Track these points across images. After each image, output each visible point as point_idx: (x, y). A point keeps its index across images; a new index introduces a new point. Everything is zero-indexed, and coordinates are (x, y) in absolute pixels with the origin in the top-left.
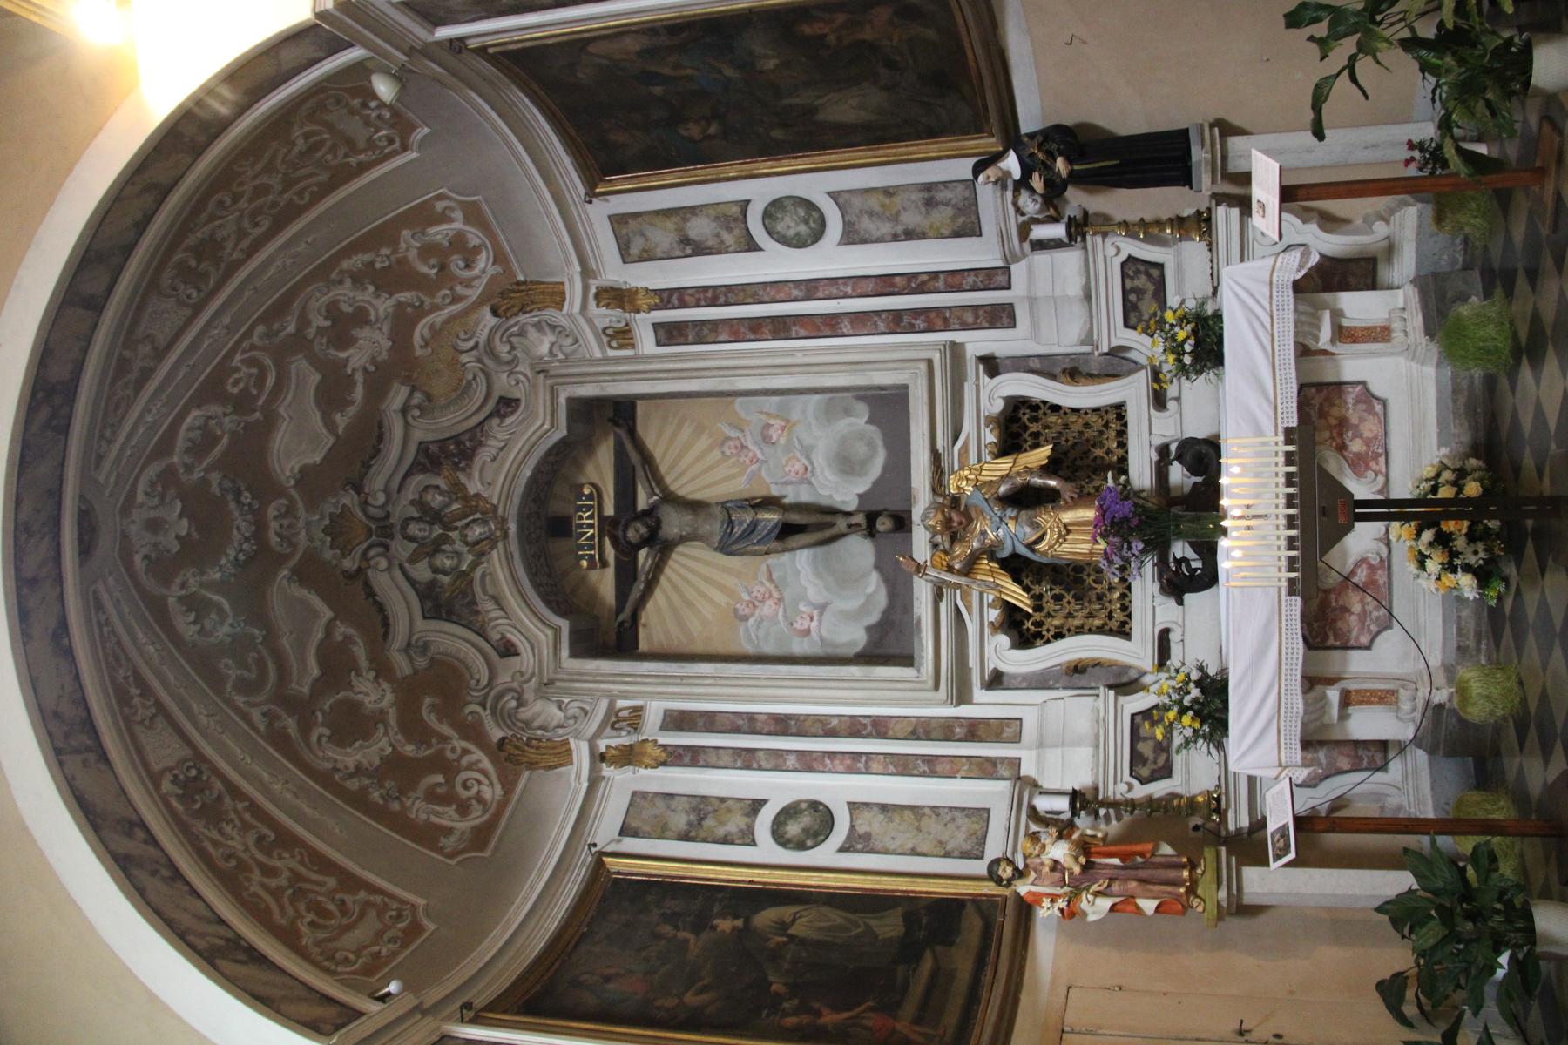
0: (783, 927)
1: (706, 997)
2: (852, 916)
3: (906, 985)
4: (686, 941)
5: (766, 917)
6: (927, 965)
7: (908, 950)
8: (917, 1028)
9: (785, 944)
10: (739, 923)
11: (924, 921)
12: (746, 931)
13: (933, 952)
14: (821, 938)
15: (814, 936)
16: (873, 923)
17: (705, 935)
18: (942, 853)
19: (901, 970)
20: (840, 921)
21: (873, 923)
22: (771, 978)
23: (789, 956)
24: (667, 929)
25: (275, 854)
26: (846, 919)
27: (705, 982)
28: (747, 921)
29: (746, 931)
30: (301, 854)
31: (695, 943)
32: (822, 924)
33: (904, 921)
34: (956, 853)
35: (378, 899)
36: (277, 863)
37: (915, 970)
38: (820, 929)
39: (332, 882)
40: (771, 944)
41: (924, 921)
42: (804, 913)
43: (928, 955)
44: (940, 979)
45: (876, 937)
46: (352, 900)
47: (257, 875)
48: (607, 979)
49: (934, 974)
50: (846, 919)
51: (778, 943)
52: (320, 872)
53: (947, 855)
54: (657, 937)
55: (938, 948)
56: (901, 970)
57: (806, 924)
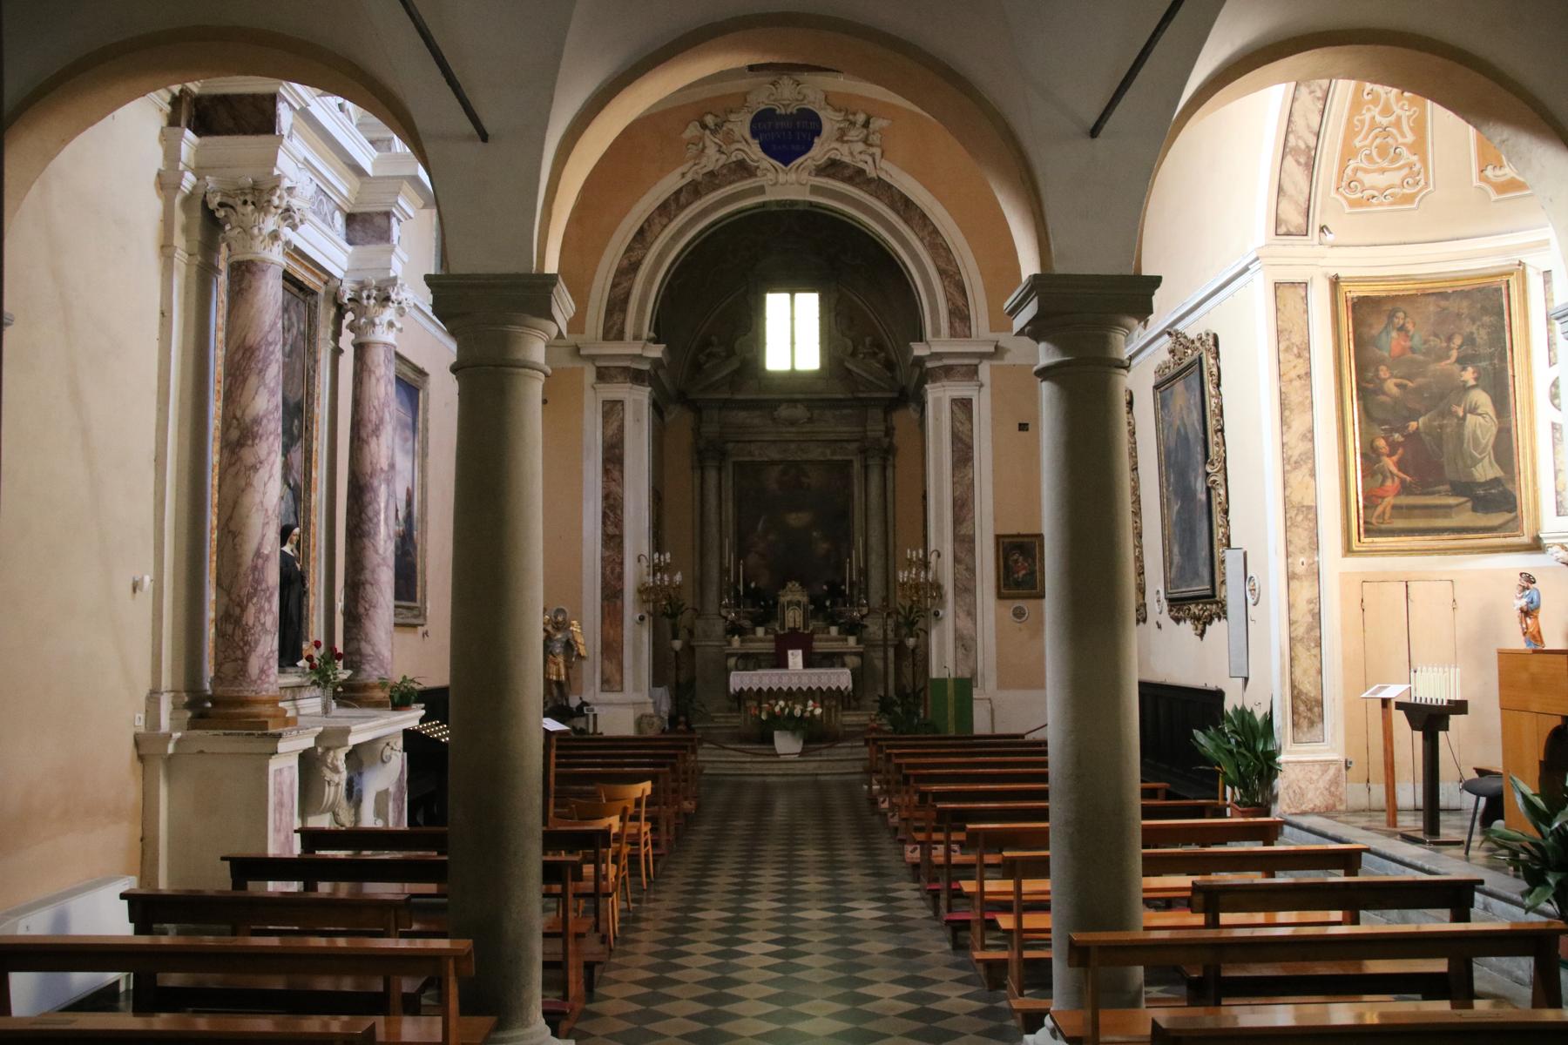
0: (1473, 410)
1: (1395, 391)
2: (1490, 447)
3: (1433, 493)
4: (1448, 357)
5: (1482, 398)
6: (1452, 501)
7: (1465, 488)
8: (1388, 509)
9: (1457, 417)
10: (1472, 382)
11: (1493, 491)
12: (1466, 389)
13: (1466, 502)
14: (1466, 437)
15: (1468, 430)
16: (1486, 460)
17: (1457, 367)
18: (1559, 489)
19: (1447, 487)
20: (1484, 442)
21: (1486, 460)
22: (1421, 420)
23: (1445, 422)
24: (1458, 341)
25: (1400, 104)
26: (1487, 445)
27: (1410, 384)
28: (1473, 387)
29: (1466, 389)
30: (1415, 112)
31: (1449, 364)
32: (1479, 432)
33: (1491, 480)
34: (1560, 499)
35: (1418, 166)
36: (1395, 108)
37: (1447, 495)
38: (1474, 432)
39: (1410, 138)
40: (1455, 408)
41: (1493, 491)
42: (1488, 418)
43: (1462, 499)
44: (1447, 510)
45: (1475, 466)
46: (1407, 156)
47: (1376, 111)
48: (1402, 329)
49: (1450, 507)
50: (1487, 445)
51: (1456, 412)
52: (1411, 128)
53: (1557, 493)
54: (1450, 339)
55: (1469, 505)
56: (1447, 487)
57: (1481, 424)
